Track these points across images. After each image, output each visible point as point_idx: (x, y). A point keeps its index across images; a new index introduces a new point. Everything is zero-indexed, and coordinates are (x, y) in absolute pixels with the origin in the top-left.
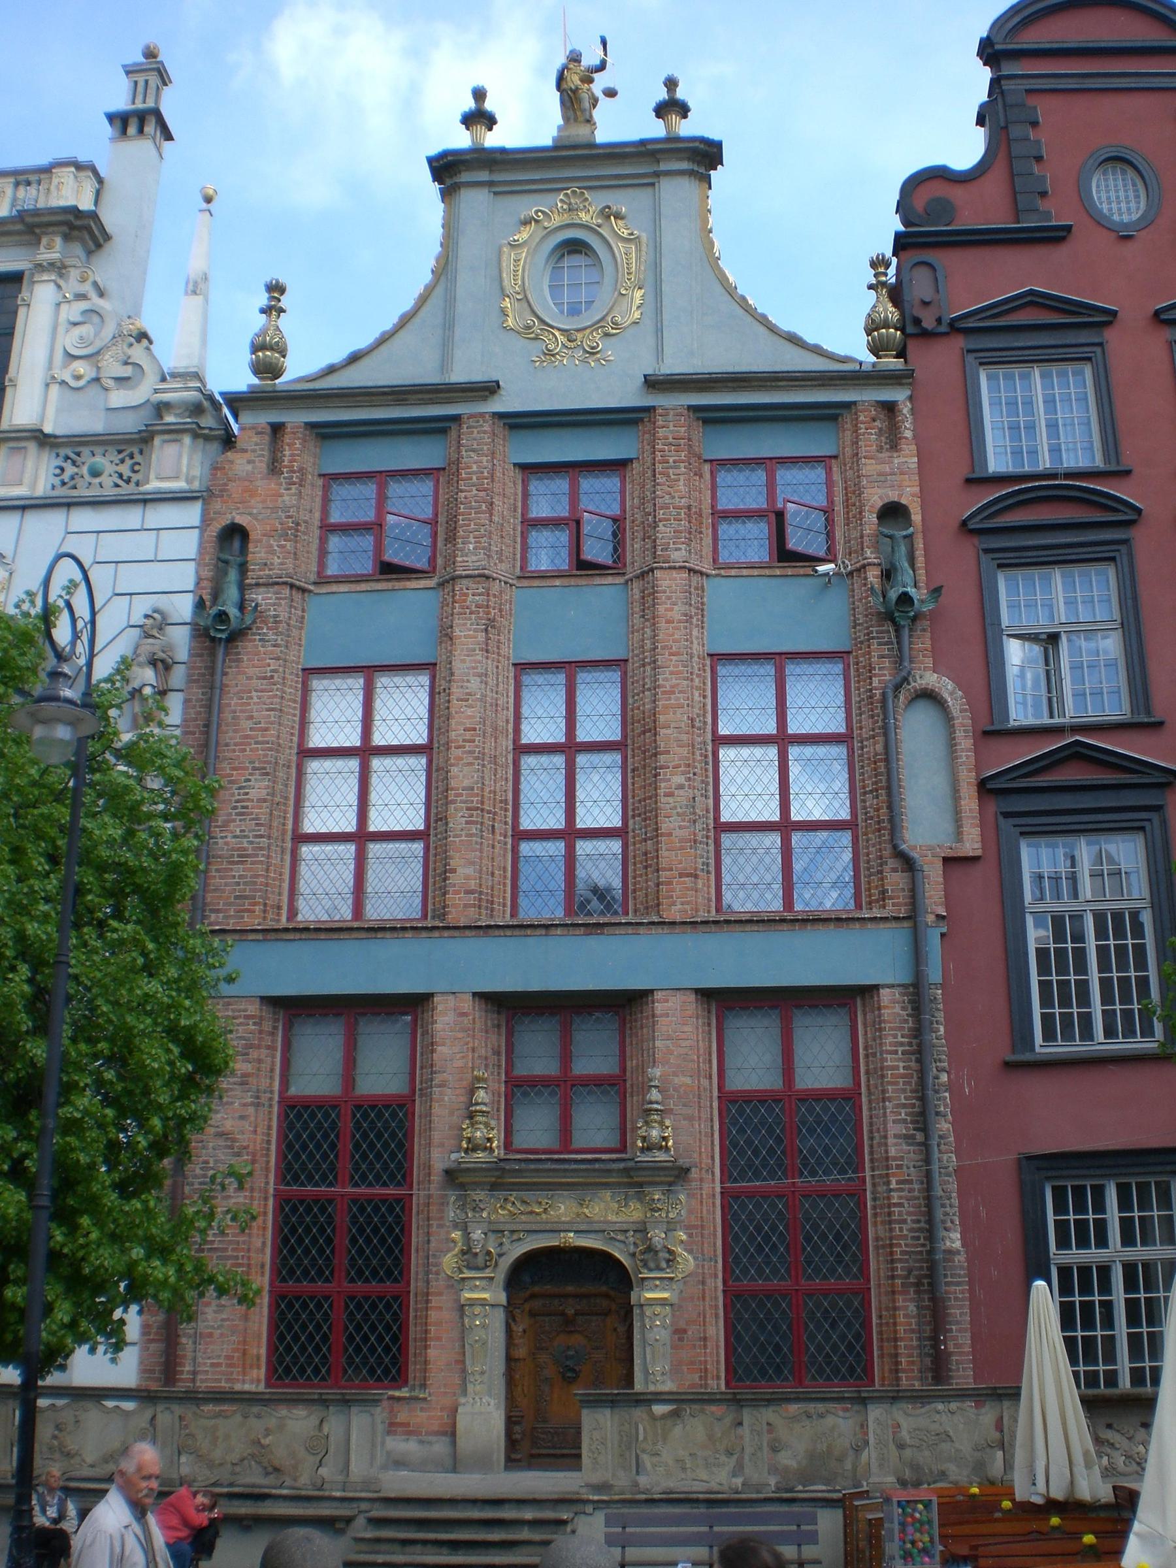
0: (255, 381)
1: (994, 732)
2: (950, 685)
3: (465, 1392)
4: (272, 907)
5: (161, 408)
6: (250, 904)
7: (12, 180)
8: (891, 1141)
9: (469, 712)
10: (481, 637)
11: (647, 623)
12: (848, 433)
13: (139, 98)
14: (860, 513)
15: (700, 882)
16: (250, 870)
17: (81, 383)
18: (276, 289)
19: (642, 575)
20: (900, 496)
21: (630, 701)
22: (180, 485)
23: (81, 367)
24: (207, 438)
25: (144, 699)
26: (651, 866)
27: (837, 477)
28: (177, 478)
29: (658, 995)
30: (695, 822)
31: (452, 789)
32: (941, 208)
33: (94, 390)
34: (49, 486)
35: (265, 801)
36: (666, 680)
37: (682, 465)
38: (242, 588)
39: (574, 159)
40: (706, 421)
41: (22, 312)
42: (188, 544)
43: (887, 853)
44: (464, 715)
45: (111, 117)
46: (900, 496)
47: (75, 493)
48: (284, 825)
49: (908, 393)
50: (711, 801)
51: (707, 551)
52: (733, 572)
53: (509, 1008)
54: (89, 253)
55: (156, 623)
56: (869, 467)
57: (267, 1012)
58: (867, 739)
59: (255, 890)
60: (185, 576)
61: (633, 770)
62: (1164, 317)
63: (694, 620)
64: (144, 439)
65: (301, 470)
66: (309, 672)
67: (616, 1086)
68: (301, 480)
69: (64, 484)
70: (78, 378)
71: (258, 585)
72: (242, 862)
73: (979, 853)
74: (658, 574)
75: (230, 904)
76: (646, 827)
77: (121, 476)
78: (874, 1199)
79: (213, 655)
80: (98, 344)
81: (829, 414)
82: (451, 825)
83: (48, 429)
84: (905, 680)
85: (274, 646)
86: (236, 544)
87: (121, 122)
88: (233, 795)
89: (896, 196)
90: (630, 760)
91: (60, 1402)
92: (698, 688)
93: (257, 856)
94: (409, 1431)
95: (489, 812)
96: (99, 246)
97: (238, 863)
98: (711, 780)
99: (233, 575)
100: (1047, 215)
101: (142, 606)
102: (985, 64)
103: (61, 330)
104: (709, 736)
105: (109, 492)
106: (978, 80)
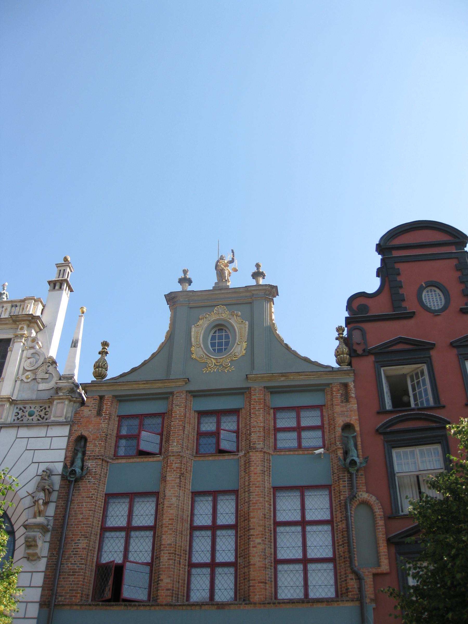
1: (392, 515)
4: (85, 595)
6: (75, 593)
7: (10, 305)
9: (171, 512)
11: (247, 475)
12: (329, 396)
13: (61, 276)
14: (334, 428)
15: (267, 585)
16: (77, 578)
17: (29, 380)
18: (105, 344)
20: (350, 420)
21: (239, 507)
22: (62, 419)
24: (75, 402)
26: (246, 579)
27: (325, 414)
30: (265, 559)
31: (163, 545)
32: (364, 308)
33: (34, 383)
34: (13, 420)
35: (85, 549)
36: (254, 498)
37: (261, 410)
38: (83, 461)
39: (222, 295)
40: (272, 393)
42: (63, 443)
43: (349, 571)
44: (169, 513)
45: (50, 282)
46: (350, 420)
48: (93, 559)
49: (353, 379)
50: (273, 550)
51: (272, 444)
52: (282, 453)
55: (48, 473)
56: (338, 409)
58: (339, 522)
59: (78, 587)
60: (60, 456)
61: (240, 537)
62: (454, 345)
63: (266, 473)
64: (50, 401)
65: (110, 414)
68: (110, 418)
69: (18, 419)
71: (89, 459)
72: (74, 575)
73: (388, 570)
75: (68, 593)
76: (244, 561)
77: (40, 416)
79: (69, 488)
80: (37, 366)
82: (161, 560)
85: (94, 484)
86: (83, 443)
88: (72, 546)
89: (345, 304)
90: (239, 533)
92: (267, 501)
93: (80, 572)
95: (178, 555)
97: (72, 575)
98: (273, 541)
99: (80, 455)
100: (405, 308)
102: (379, 254)
103: (23, 360)
104: (272, 522)
106: (376, 260)
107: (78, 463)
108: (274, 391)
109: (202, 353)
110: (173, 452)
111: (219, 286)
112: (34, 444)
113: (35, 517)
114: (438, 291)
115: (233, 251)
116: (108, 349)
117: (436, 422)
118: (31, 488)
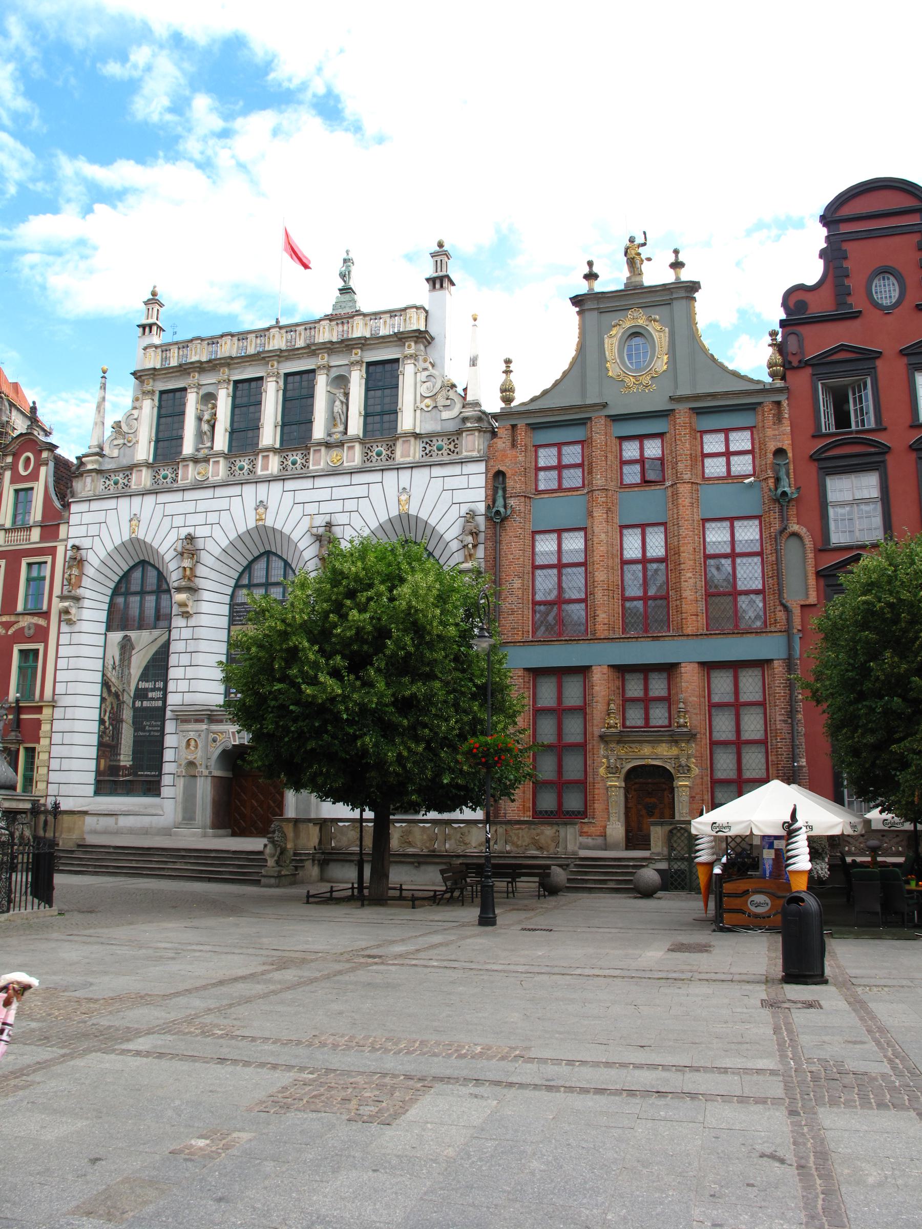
0: (503, 405)
2: (804, 530)
3: (609, 821)
5: (465, 420)
8: (778, 722)
9: (602, 549)
10: (605, 516)
13: (439, 269)
18: (508, 362)
19: (672, 485)
23: (428, 401)
24: (485, 432)
25: (469, 549)
27: (756, 436)
28: (473, 451)
29: (683, 665)
38: (505, 498)
40: (698, 414)
41: (401, 377)
42: (481, 480)
43: (778, 603)
44: (600, 550)
45: (428, 280)
47: (431, 459)
53: (622, 670)
54: (426, 347)
56: (769, 432)
57: (526, 674)
60: (481, 494)
64: (459, 433)
66: (534, 533)
67: (668, 700)
70: (428, 407)
74: (678, 485)
79: (495, 528)
81: (752, 408)
83: (418, 431)
84: (785, 529)
86: (501, 479)
87: (432, 281)
91: (462, 825)
94: (588, 835)
96: (429, 343)
99: (500, 493)
100: (851, 306)
101: (464, 509)
103: (418, 385)
105: (446, 458)
106: (819, 236)
107: (500, 502)
108: (699, 412)
109: (618, 370)
110: (597, 486)
112: (451, 483)
113: (466, 561)
114: (891, 278)
115: (645, 233)
116: (512, 367)
117: (875, 447)
118: (455, 531)
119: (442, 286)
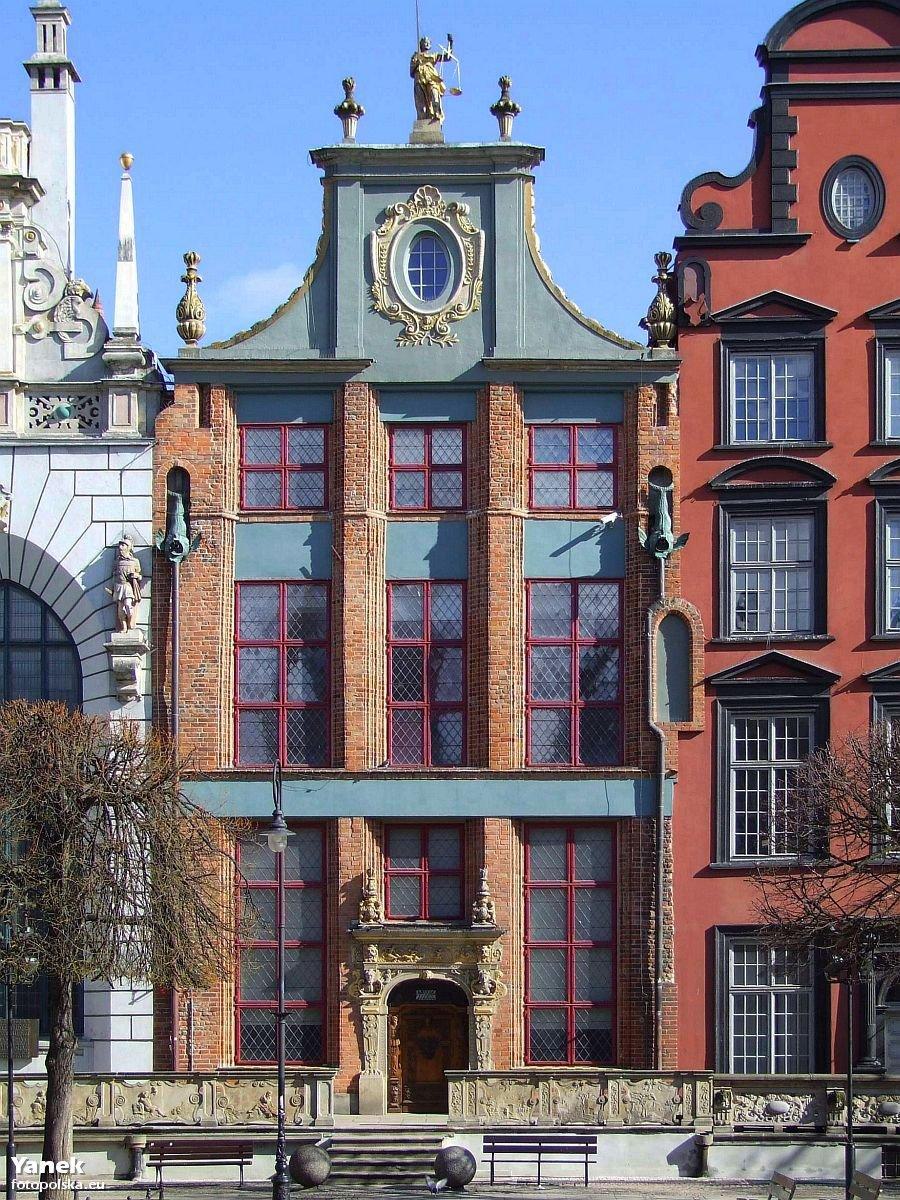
13: (50, 45)
21: (469, 611)
26: (483, 731)
27: (621, 440)
32: (712, 212)
36: (494, 599)
38: (187, 519)
56: (644, 438)
60: (143, 508)
61: (471, 662)
71: (199, 517)
72: (203, 725)
78: (622, 951)
102: (761, 65)
107: (180, 526)
111: (423, 134)
112: (86, 483)
114: (864, 179)
119: (56, 84)
